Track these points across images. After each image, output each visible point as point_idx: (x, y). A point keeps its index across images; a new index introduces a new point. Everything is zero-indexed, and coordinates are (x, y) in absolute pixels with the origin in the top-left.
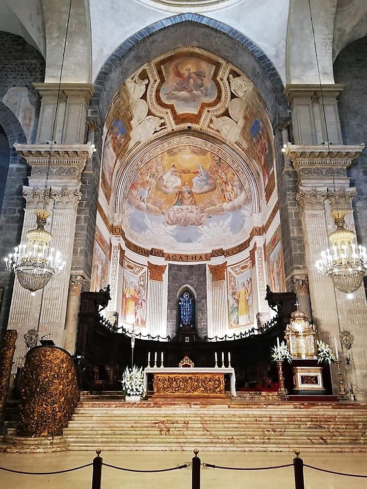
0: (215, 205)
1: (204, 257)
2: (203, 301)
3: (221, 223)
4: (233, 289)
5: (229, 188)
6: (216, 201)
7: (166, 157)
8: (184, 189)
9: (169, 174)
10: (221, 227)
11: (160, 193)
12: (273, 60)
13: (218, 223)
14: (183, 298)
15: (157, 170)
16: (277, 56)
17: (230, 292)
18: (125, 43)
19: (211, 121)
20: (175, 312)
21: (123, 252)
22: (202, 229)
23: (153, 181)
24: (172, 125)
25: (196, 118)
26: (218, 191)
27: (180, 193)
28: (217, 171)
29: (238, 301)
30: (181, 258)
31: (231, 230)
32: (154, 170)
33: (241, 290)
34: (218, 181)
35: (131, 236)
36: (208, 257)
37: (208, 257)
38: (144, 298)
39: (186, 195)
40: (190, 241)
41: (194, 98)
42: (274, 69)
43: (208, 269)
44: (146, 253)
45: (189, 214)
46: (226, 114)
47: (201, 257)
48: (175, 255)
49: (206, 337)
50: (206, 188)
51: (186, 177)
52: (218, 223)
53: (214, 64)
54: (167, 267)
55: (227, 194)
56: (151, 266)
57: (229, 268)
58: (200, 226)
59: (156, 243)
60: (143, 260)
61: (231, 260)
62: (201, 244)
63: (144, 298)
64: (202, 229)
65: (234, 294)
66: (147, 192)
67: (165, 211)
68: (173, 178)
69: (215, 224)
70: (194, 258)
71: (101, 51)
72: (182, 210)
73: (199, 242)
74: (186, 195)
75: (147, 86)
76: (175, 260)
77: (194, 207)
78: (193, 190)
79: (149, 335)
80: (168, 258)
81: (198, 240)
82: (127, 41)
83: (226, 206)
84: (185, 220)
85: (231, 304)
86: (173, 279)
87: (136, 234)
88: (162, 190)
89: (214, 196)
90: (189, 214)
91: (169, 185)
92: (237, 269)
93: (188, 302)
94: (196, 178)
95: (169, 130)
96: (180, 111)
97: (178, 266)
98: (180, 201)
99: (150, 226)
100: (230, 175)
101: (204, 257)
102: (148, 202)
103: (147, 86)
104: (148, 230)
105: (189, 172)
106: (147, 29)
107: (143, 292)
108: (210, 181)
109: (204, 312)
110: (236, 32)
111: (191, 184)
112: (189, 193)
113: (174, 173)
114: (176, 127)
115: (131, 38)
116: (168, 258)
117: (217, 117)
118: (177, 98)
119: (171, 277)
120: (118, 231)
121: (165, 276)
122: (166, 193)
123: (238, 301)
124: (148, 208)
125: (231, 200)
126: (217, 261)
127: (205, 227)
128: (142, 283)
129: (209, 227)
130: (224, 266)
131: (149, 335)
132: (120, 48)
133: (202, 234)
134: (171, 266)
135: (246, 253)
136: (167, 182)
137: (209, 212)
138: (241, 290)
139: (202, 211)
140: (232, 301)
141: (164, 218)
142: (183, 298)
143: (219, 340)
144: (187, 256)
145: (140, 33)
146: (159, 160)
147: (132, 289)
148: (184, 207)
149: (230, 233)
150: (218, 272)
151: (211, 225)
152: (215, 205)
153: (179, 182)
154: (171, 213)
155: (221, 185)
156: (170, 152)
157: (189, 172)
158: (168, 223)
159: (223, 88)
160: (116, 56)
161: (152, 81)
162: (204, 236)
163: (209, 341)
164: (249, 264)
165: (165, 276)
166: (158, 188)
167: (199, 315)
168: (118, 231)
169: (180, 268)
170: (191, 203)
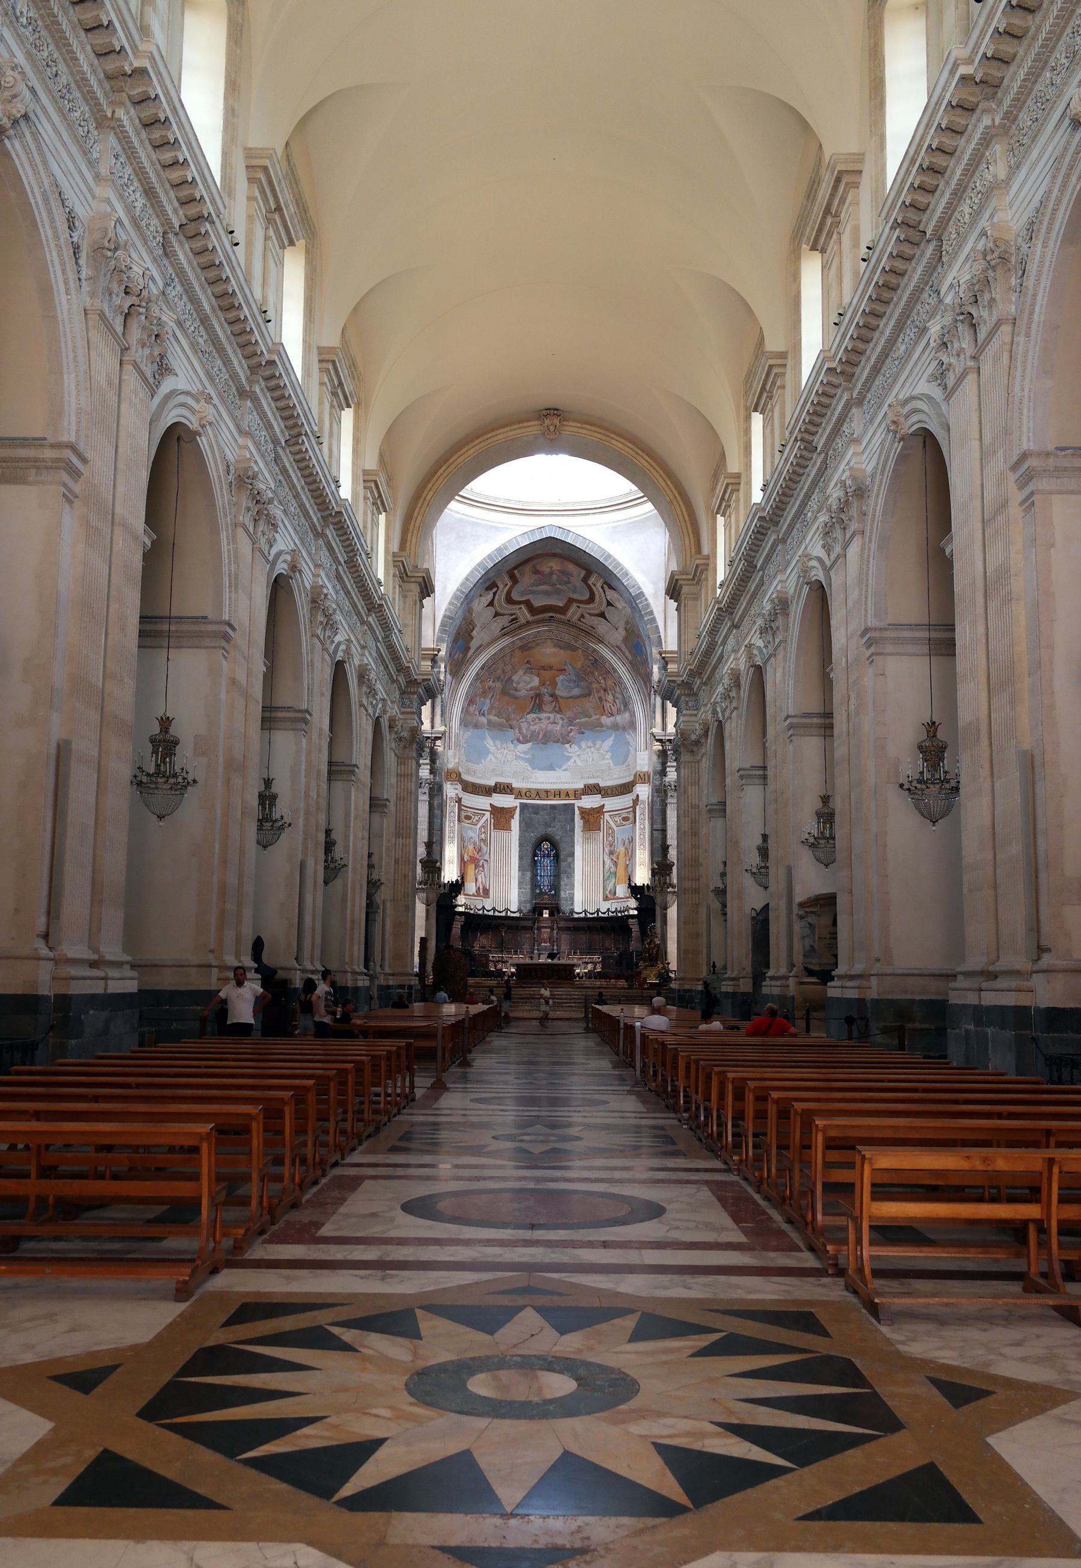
0: (590, 717)
1: (571, 794)
2: (569, 859)
3: (599, 743)
4: (611, 846)
5: (610, 698)
6: (591, 711)
7: (518, 653)
8: (544, 690)
9: (521, 672)
10: (598, 749)
11: (507, 698)
12: (651, 601)
13: (594, 743)
14: (540, 850)
15: (503, 671)
16: (655, 595)
17: (607, 850)
18: (472, 572)
19: (582, 616)
20: (529, 874)
21: (459, 801)
22: (570, 750)
23: (498, 685)
24: (524, 614)
25: (563, 610)
26: (593, 700)
27: (538, 696)
28: (593, 673)
29: (616, 864)
30: (539, 794)
31: (612, 758)
32: (499, 672)
33: (621, 849)
34: (594, 686)
35: (468, 772)
36: (577, 794)
37: (577, 794)
38: (486, 857)
39: (547, 698)
40: (551, 768)
41: (558, 592)
42: (651, 613)
43: (577, 812)
44: (488, 791)
45: (550, 727)
46: (602, 615)
47: (568, 795)
48: (529, 790)
49: (572, 912)
50: (576, 692)
51: (547, 674)
52: (594, 743)
53: (585, 569)
54: (518, 809)
55: (607, 705)
56: (495, 811)
57: (607, 816)
58: (567, 745)
59: (501, 775)
60: (483, 802)
61: (612, 803)
62: (568, 773)
63: (486, 857)
64: (570, 750)
65: (611, 853)
66: (488, 701)
67: (514, 723)
68: (527, 678)
69: (590, 744)
70: (558, 794)
71: (445, 587)
72: (540, 719)
73: (566, 770)
74: (547, 698)
75: (495, 594)
76: (529, 798)
77: (559, 716)
78: (558, 692)
79: (494, 909)
80: (519, 794)
81: (564, 767)
82: (475, 569)
83: (606, 720)
84: (545, 735)
85: (607, 867)
86: (525, 825)
87: (474, 767)
88: (509, 695)
89: (590, 704)
90: (550, 727)
91: (521, 685)
92: (617, 819)
93: (548, 856)
94: (561, 677)
95: (523, 621)
96: (538, 603)
97: (533, 806)
98: (538, 706)
99: (492, 749)
100: (610, 683)
101: (571, 794)
102: (489, 714)
103: (495, 594)
104: (490, 756)
105: (551, 668)
106: (499, 550)
107: (485, 849)
108: (582, 683)
109: (571, 875)
110: (609, 556)
111: (554, 684)
112: (552, 696)
113: (529, 670)
114: (530, 618)
115: (479, 565)
116: (519, 794)
117: (591, 615)
118: (533, 592)
119: (523, 824)
120: (454, 776)
121: (515, 823)
122: (516, 698)
123: (616, 864)
124: (490, 722)
125: (612, 715)
126: (589, 802)
127: (575, 748)
128: (483, 836)
129: (580, 747)
130: (600, 810)
131: (494, 909)
132: (467, 579)
133: (569, 758)
134: (523, 807)
135: (625, 801)
136: (518, 683)
137: (580, 725)
138: (621, 849)
139: (571, 722)
140: (608, 862)
141: (511, 734)
142: (540, 850)
143: (589, 916)
144: (547, 792)
145: (489, 556)
146: (508, 658)
147: (471, 847)
148: (543, 715)
149: (611, 761)
150: (593, 819)
151: (583, 744)
152: (590, 717)
153: (536, 682)
154: (524, 726)
155: (598, 692)
156: (525, 648)
157: (551, 668)
158: (519, 741)
159: (596, 592)
160: (462, 592)
161: (501, 586)
162: (572, 761)
163: (576, 916)
164: (631, 816)
165: (515, 823)
166: (504, 692)
167: (564, 881)
168: (454, 776)
169: (536, 809)
170: (554, 711)
